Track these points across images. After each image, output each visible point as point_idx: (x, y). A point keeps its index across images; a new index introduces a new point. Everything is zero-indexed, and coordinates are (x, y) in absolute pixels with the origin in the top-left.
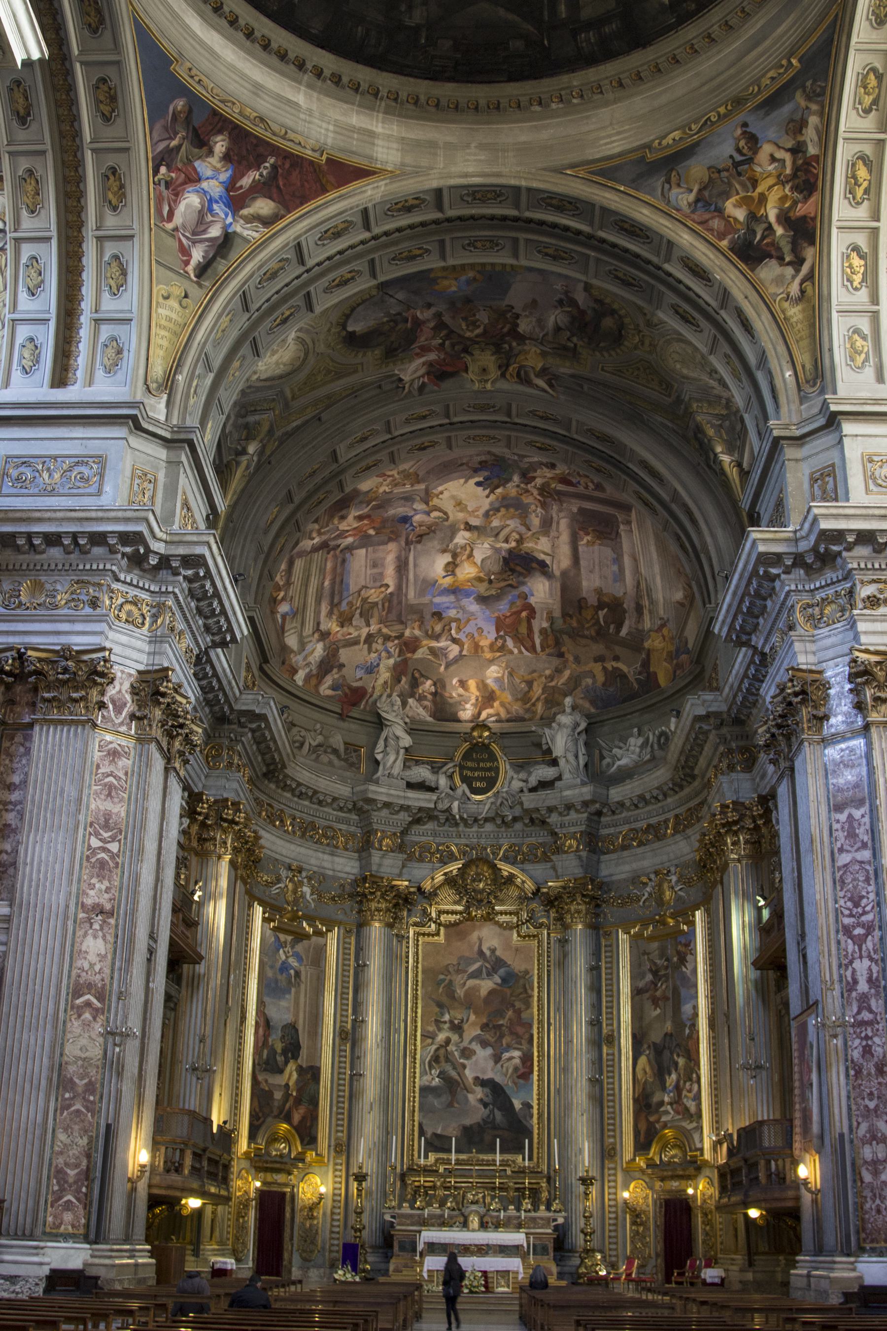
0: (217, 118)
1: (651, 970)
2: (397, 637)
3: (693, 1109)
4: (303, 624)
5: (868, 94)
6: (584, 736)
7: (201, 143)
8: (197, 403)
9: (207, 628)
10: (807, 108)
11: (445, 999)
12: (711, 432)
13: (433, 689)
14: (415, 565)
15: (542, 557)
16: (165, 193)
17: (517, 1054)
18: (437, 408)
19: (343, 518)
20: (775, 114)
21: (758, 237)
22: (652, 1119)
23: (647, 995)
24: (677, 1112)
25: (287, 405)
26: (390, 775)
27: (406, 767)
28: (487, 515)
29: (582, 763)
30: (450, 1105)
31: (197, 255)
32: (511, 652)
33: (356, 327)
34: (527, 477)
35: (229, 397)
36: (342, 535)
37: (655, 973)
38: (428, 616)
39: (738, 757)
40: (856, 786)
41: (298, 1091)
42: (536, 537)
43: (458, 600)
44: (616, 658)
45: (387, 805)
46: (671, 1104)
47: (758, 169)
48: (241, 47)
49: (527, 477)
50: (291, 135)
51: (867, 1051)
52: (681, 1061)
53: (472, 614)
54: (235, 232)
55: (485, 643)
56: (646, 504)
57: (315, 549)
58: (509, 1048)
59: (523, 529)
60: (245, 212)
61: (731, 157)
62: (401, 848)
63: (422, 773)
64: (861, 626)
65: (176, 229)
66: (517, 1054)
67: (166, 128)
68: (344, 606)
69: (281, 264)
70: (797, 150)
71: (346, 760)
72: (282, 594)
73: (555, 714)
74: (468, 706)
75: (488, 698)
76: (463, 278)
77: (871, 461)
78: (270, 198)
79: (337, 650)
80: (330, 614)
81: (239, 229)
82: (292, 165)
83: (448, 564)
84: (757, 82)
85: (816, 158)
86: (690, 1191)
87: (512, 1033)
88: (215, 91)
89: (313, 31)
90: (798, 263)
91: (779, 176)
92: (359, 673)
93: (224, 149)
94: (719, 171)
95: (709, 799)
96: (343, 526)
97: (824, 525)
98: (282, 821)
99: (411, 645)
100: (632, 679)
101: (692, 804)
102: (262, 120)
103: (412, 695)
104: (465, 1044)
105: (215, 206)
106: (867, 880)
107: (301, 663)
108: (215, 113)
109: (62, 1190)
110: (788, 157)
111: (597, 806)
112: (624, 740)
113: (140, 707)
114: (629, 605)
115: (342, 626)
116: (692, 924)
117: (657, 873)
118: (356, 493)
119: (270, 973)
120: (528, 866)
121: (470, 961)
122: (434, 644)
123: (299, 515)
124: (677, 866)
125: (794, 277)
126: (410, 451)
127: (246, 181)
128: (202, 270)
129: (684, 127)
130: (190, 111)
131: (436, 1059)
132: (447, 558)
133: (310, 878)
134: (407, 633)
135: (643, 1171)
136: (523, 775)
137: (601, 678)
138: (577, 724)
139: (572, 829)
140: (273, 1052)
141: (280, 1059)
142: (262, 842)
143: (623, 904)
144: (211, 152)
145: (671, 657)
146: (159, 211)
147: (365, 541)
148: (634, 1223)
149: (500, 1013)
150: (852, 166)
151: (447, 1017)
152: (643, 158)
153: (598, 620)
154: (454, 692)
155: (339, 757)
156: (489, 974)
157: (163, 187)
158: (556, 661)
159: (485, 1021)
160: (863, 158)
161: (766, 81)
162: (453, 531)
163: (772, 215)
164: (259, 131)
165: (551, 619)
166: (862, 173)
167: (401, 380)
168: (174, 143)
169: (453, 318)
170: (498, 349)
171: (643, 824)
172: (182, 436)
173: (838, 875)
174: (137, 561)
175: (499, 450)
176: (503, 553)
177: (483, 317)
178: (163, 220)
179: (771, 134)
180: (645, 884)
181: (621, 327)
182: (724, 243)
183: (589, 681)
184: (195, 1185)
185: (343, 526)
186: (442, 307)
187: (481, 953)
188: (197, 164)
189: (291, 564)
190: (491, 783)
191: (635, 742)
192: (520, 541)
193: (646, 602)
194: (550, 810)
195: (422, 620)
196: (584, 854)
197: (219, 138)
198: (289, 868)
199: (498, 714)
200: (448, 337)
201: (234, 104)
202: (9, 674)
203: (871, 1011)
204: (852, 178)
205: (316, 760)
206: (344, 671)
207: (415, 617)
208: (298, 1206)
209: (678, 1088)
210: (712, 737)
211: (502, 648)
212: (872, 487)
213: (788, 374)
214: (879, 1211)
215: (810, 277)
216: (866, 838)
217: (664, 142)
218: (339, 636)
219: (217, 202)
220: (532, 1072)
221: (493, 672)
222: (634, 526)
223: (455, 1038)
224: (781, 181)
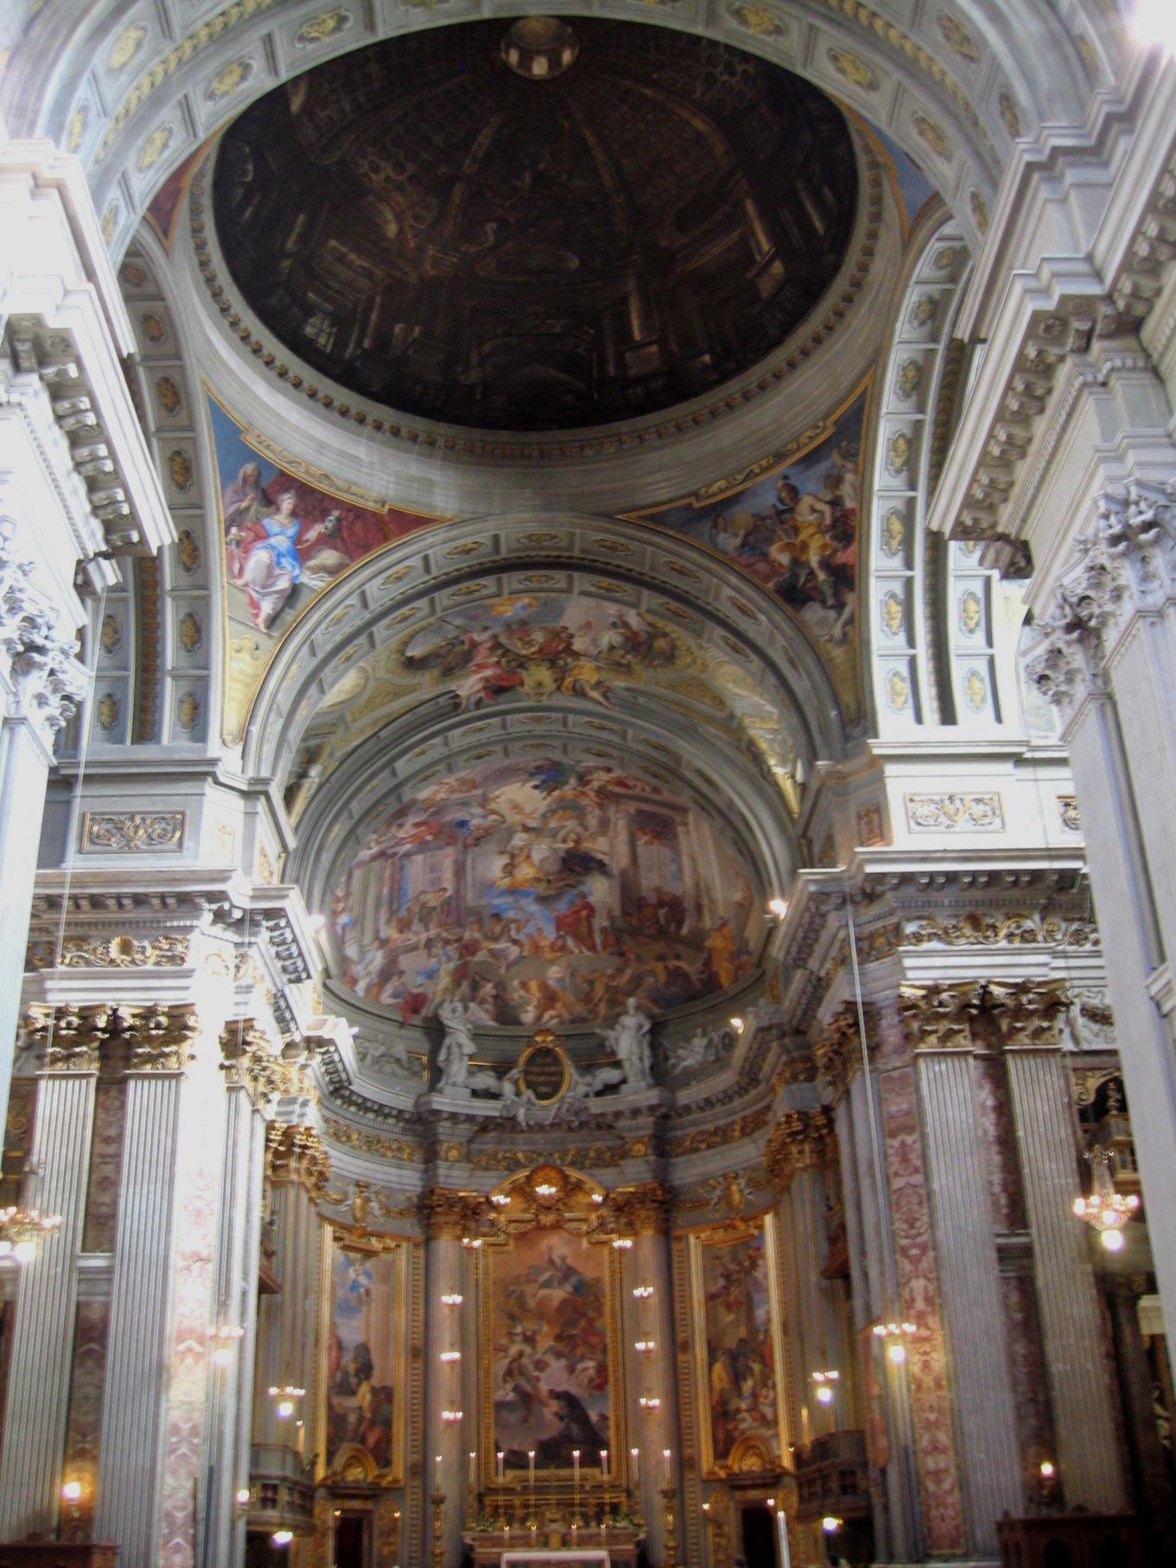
1: (723, 1275)
2: (456, 941)
3: (768, 1411)
4: (362, 933)
6: (648, 1038)
8: (269, 749)
9: (284, 969)
11: (516, 1310)
12: (764, 746)
13: (494, 992)
14: (474, 868)
15: (600, 856)
16: (236, 551)
17: (591, 1364)
18: (495, 721)
19: (400, 826)
20: (811, 471)
21: (802, 581)
22: (730, 1426)
23: (719, 1301)
24: (754, 1419)
25: (347, 729)
26: (454, 1084)
27: (471, 1072)
28: (544, 816)
29: (647, 1063)
30: (525, 1420)
31: (267, 607)
32: (571, 952)
33: (414, 652)
34: (583, 780)
35: (295, 734)
36: (400, 842)
37: (727, 1276)
38: (486, 916)
39: (800, 1066)
40: (908, 1113)
41: (375, 1411)
42: (593, 837)
43: (517, 901)
44: (678, 957)
45: (453, 1117)
46: (747, 1411)
47: (800, 518)
48: (306, 407)
49: (583, 780)
50: (354, 489)
51: (926, 1365)
52: (757, 1367)
53: (531, 914)
55: (543, 943)
56: (703, 808)
57: (374, 858)
58: (583, 1358)
59: (579, 829)
60: (311, 563)
62: (467, 1157)
63: (486, 1080)
64: (908, 962)
65: (246, 585)
66: (591, 1364)
67: (236, 492)
68: (403, 913)
70: (835, 503)
71: (408, 1069)
72: (341, 905)
73: (618, 1015)
74: (530, 1008)
75: (550, 999)
76: (519, 604)
77: (912, 800)
78: (335, 549)
79: (396, 957)
80: (389, 920)
81: (306, 578)
83: (506, 866)
84: (796, 439)
85: (853, 511)
86: (771, 1502)
87: (586, 1343)
90: (840, 606)
91: (819, 525)
92: (420, 980)
94: (763, 519)
95: (775, 1107)
96: (401, 834)
97: (871, 869)
98: (349, 1137)
99: (469, 949)
100: (694, 978)
101: (758, 1107)
102: (326, 476)
103: (473, 999)
104: (539, 1356)
105: (283, 560)
106: (920, 1203)
107: (362, 973)
108: (282, 474)
109: (172, 1533)
110: (826, 509)
111: (663, 1110)
112: (688, 1040)
113: (227, 1057)
114: (688, 904)
115: (401, 931)
116: (761, 1227)
117: (725, 1176)
118: (414, 802)
119: (340, 1293)
120: (596, 1171)
121: (539, 1270)
122: (494, 946)
123: (360, 831)
124: (745, 1169)
125: (837, 620)
126: (467, 760)
127: (312, 535)
128: (272, 621)
129: (729, 477)
130: (259, 475)
131: (509, 1373)
132: (505, 860)
133: (377, 1193)
134: (467, 936)
135: (721, 1480)
136: (588, 1079)
137: (663, 978)
138: (640, 1027)
139: (641, 1133)
140: (346, 1374)
141: (353, 1380)
142: (332, 1162)
143: (693, 1208)
144: (278, 510)
145: (732, 957)
146: (230, 568)
147: (423, 846)
148: (716, 1535)
149: (574, 1323)
150: (887, 520)
151: (519, 1329)
152: (690, 505)
153: (657, 922)
154: (516, 995)
155: (402, 1066)
156: (560, 1283)
157: (233, 546)
158: (617, 961)
159: (557, 1330)
160: (895, 513)
161: (804, 440)
162: (510, 833)
163: (814, 559)
164: (323, 487)
165: (611, 918)
166: (897, 526)
167: (457, 696)
168: (244, 505)
169: (509, 638)
170: (553, 664)
171: (710, 1127)
172: (259, 788)
173: (894, 1197)
174: (220, 916)
175: (557, 756)
176: (562, 854)
177: (539, 637)
178: (234, 577)
179: (811, 486)
180: (714, 1188)
181: (674, 648)
182: (771, 585)
183: (651, 980)
184: (288, 1516)
185: (401, 834)
186: (497, 629)
187: (551, 1262)
188: (266, 522)
189: (350, 875)
190: (556, 1087)
191: (699, 1043)
192: (578, 841)
193: (705, 901)
194: (618, 1115)
195: (480, 921)
196: (652, 1158)
197: (286, 496)
198: (358, 1185)
199: (559, 1016)
200: (504, 655)
202: (104, 1030)
203: (928, 1328)
204: (887, 533)
205: (380, 1071)
206: (405, 978)
207: (473, 919)
208: (376, 1532)
209: (755, 1395)
210: (775, 1045)
211: (563, 948)
212: (913, 825)
213: (833, 714)
214: (943, 1520)
215: (850, 621)
216: (918, 1163)
218: (399, 943)
220: (606, 1382)
221: (554, 972)
222: (692, 827)
223: (528, 1350)
224: (821, 530)
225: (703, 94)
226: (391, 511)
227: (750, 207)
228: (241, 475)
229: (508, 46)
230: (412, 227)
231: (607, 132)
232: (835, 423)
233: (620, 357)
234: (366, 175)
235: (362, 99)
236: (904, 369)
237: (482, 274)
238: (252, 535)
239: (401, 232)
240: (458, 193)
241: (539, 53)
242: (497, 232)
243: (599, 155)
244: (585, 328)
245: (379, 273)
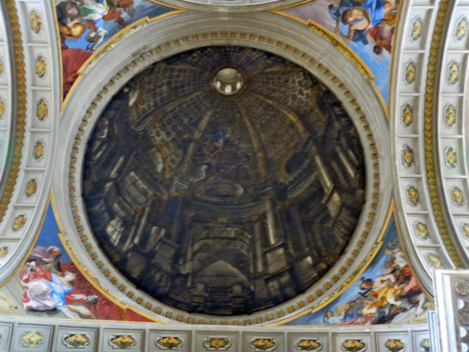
0: (72, 267)
5: (422, 232)
7: (60, 269)
10: (393, 253)
31: (33, 304)
54: (60, 311)
60: (71, 306)
61: (360, 293)
65: (27, 288)
67: (44, 252)
69: (84, 340)
81: (65, 310)
82: (106, 303)
85: (407, 266)
88: (76, 257)
89: (134, 276)
93: (71, 279)
94: (354, 301)
105: (55, 295)
108: (72, 264)
127: (78, 297)
130: (60, 255)
144: (63, 275)
157: (29, 269)
163: (391, 300)
168: (45, 259)
201: (84, 267)
217: (320, 304)
219: (56, 294)
224: (390, 286)
225: (292, 103)
226: (128, 310)
227: (318, 160)
228: (51, 247)
229: (217, 81)
230: (169, 166)
231: (254, 120)
232: (382, 240)
233: (264, 254)
234: (153, 137)
235: (158, 101)
236: (408, 191)
237: (198, 195)
238: (42, 274)
239: (164, 169)
240: (191, 148)
241: (229, 84)
242: (207, 171)
243: (251, 131)
244: (246, 234)
245: (150, 193)
